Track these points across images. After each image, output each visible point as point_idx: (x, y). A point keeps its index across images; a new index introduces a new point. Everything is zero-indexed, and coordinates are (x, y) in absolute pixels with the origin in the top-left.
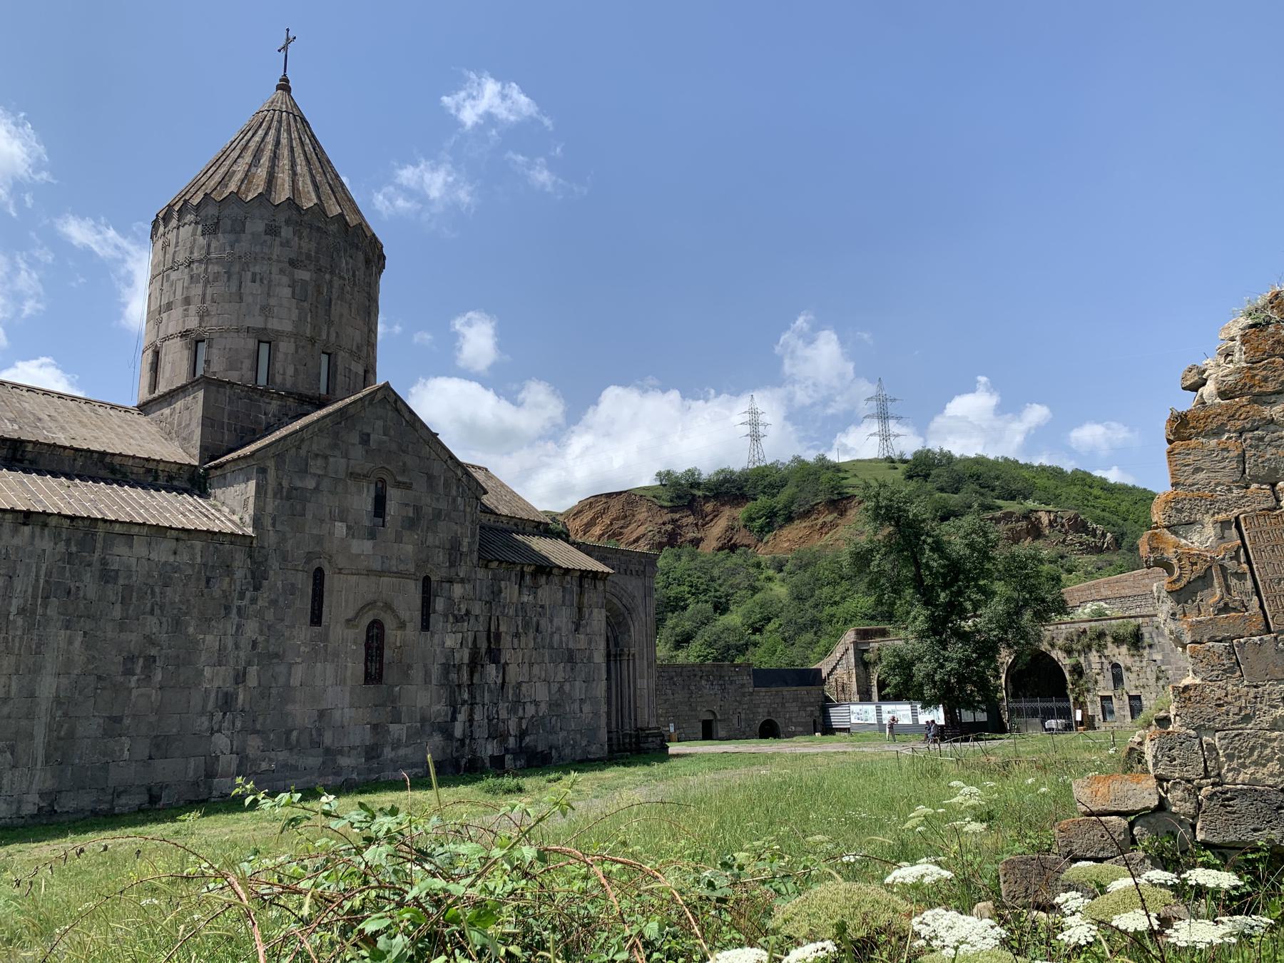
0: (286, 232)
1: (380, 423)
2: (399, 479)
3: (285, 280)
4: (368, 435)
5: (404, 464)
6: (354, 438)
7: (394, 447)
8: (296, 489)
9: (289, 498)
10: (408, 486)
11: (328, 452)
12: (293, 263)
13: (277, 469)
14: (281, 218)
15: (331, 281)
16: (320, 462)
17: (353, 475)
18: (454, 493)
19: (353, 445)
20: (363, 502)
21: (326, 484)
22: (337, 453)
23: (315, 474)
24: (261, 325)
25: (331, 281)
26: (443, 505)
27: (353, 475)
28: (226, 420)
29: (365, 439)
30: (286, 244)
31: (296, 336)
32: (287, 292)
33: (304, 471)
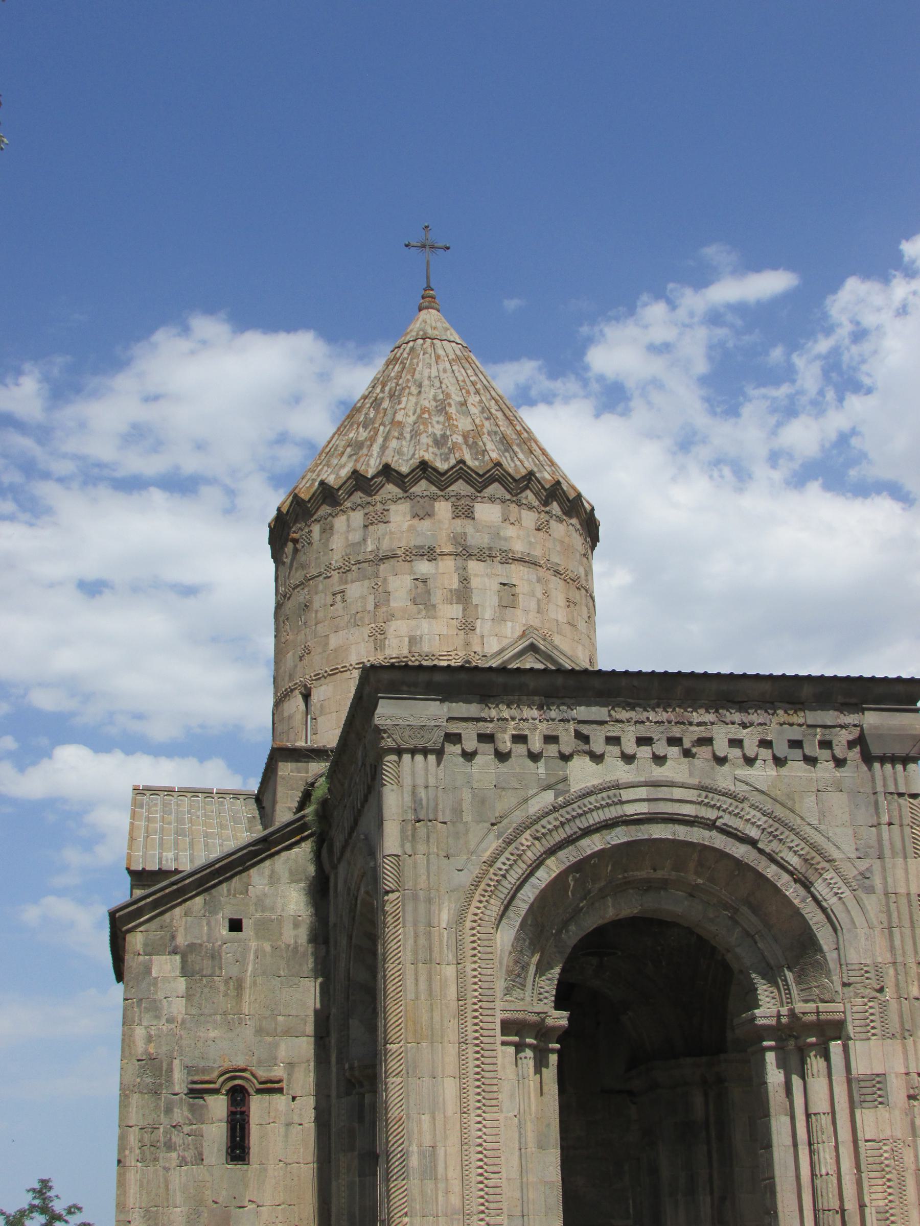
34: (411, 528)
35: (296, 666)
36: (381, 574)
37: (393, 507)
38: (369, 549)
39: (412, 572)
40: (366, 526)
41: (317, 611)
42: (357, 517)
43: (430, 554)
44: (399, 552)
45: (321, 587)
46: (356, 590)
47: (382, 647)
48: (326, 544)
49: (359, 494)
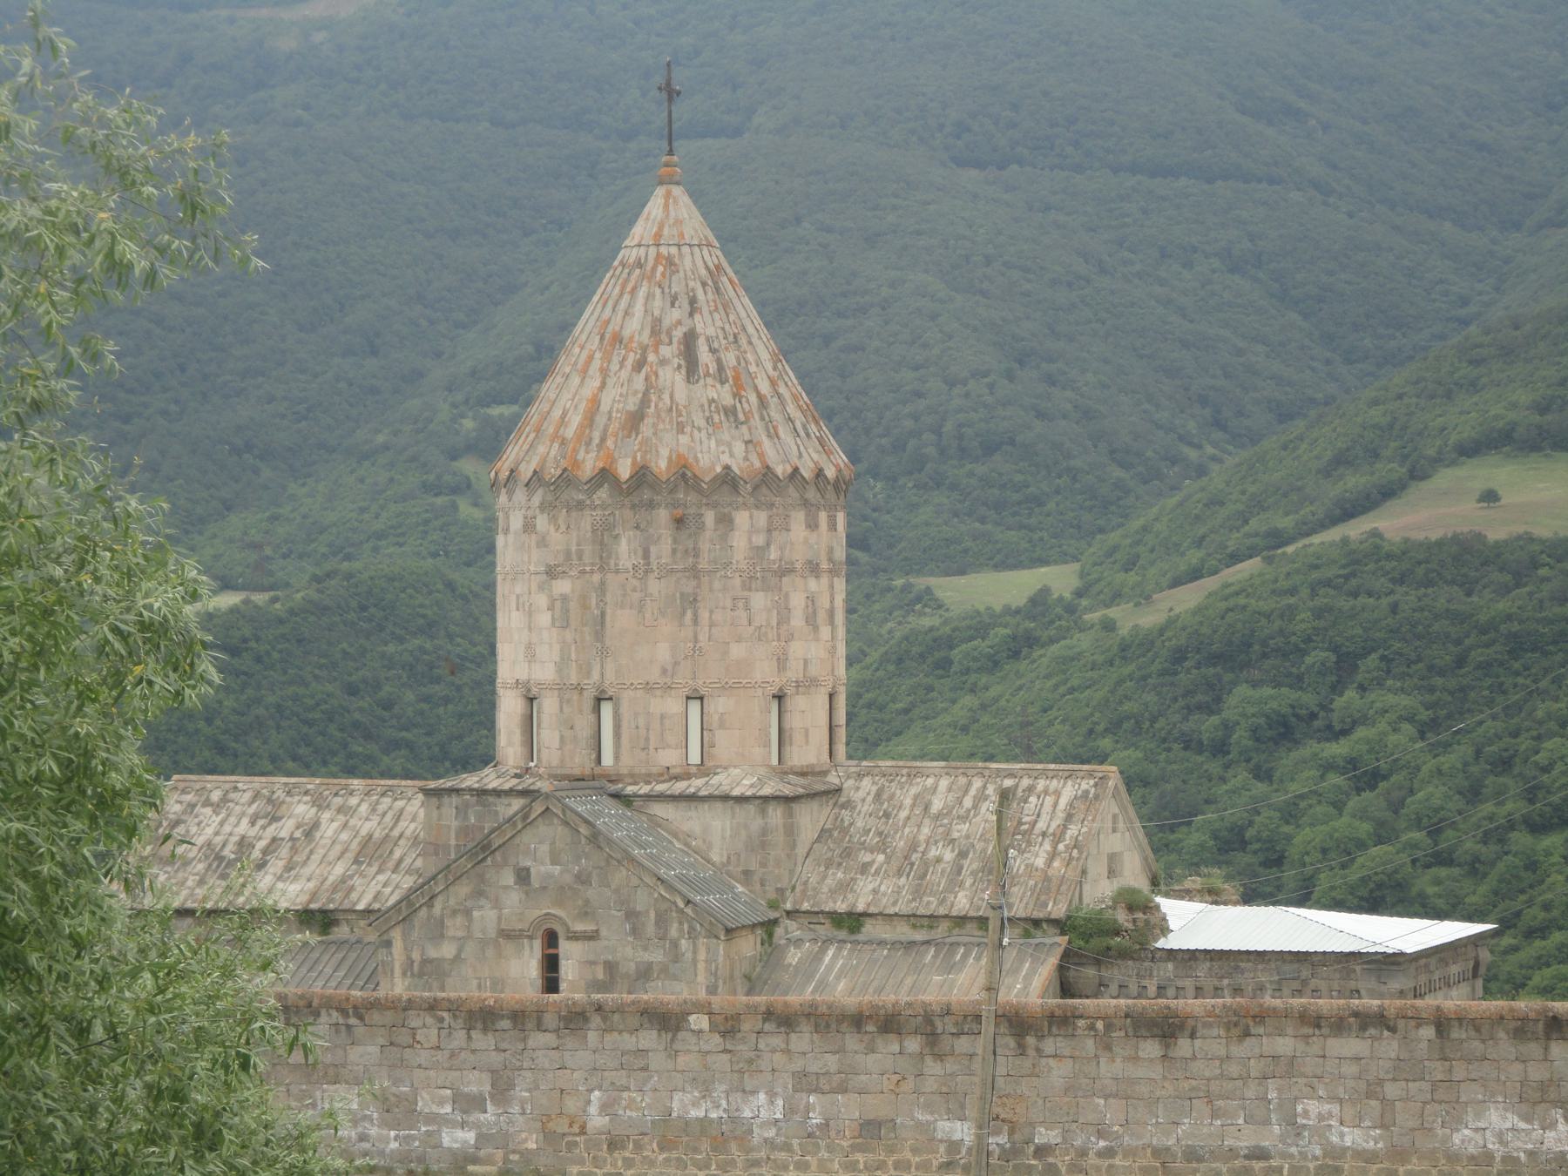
0: (542, 522)
1: (545, 848)
2: (579, 927)
3: (542, 600)
4: (528, 870)
5: (587, 902)
6: (508, 878)
7: (568, 878)
8: (430, 961)
9: (421, 975)
10: (592, 936)
11: (469, 904)
12: (552, 573)
13: (404, 941)
14: (537, 500)
15: (603, 583)
16: (459, 920)
17: (508, 935)
18: (674, 932)
19: (506, 887)
20: (526, 967)
21: (470, 950)
22: (483, 902)
23: (454, 938)
24: (523, 677)
25: (603, 583)
26: (656, 956)
27: (508, 935)
28: (453, 842)
29: (523, 876)
30: (543, 543)
31: (561, 688)
32: (544, 619)
33: (437, 932)
34: (806, 541)
35: (676, 664)
36: (785, 589)
37: (793, 514)
38: (772, 557)
39: (806, 591)
40: (769, 531)
41: (711, 612)
42: (762, 517)
43: (814, 569)
44: (798, 566)
45: (717, 585)
46: (759, 600)
47: (785, 669)
48: (724, 538)
49: (764, 490)
